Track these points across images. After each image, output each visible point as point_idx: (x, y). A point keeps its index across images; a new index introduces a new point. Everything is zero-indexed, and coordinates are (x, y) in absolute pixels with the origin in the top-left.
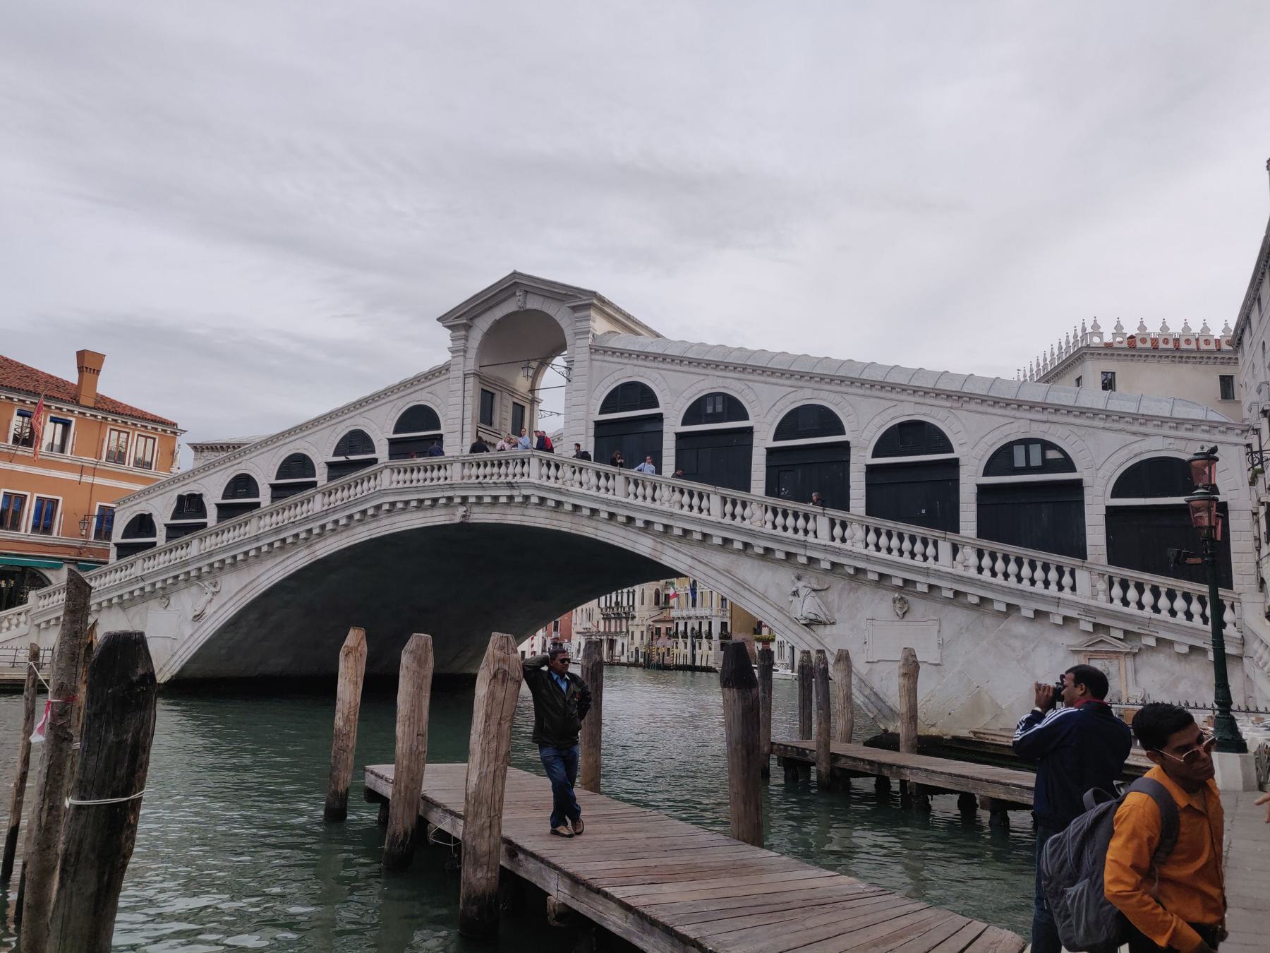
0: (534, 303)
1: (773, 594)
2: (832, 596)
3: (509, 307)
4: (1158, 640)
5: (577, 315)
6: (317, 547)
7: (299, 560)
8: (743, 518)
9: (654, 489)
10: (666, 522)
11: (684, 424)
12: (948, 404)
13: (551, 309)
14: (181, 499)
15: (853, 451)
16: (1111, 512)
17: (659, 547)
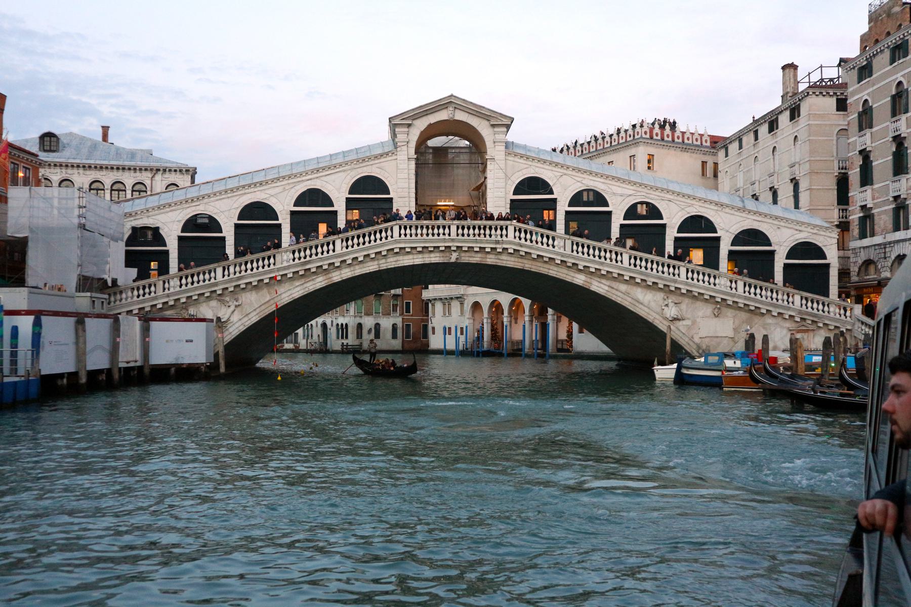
0: (460, 116)
1: (653, 304)
2: (683, 306)
3: (443, 116)
4: (824, 324)
5: (496, 129)
6: (334, 274)
7: (319, 282)
8: (641, 267)
9: (588, 247)
10: (597, 267)
11: (570, 205)
12: (716, 208)
13: (474, 122)
14: (134, 229)
15: (667, 229)
16: (786, 266)
17: (589, 280)
